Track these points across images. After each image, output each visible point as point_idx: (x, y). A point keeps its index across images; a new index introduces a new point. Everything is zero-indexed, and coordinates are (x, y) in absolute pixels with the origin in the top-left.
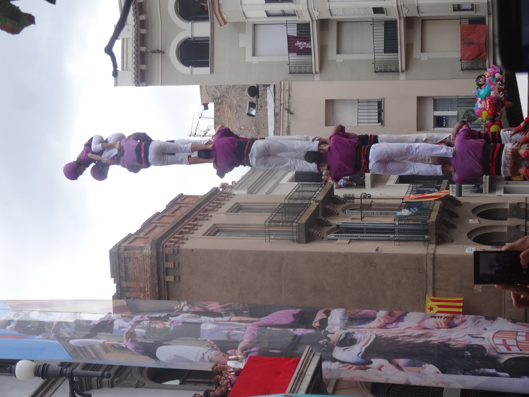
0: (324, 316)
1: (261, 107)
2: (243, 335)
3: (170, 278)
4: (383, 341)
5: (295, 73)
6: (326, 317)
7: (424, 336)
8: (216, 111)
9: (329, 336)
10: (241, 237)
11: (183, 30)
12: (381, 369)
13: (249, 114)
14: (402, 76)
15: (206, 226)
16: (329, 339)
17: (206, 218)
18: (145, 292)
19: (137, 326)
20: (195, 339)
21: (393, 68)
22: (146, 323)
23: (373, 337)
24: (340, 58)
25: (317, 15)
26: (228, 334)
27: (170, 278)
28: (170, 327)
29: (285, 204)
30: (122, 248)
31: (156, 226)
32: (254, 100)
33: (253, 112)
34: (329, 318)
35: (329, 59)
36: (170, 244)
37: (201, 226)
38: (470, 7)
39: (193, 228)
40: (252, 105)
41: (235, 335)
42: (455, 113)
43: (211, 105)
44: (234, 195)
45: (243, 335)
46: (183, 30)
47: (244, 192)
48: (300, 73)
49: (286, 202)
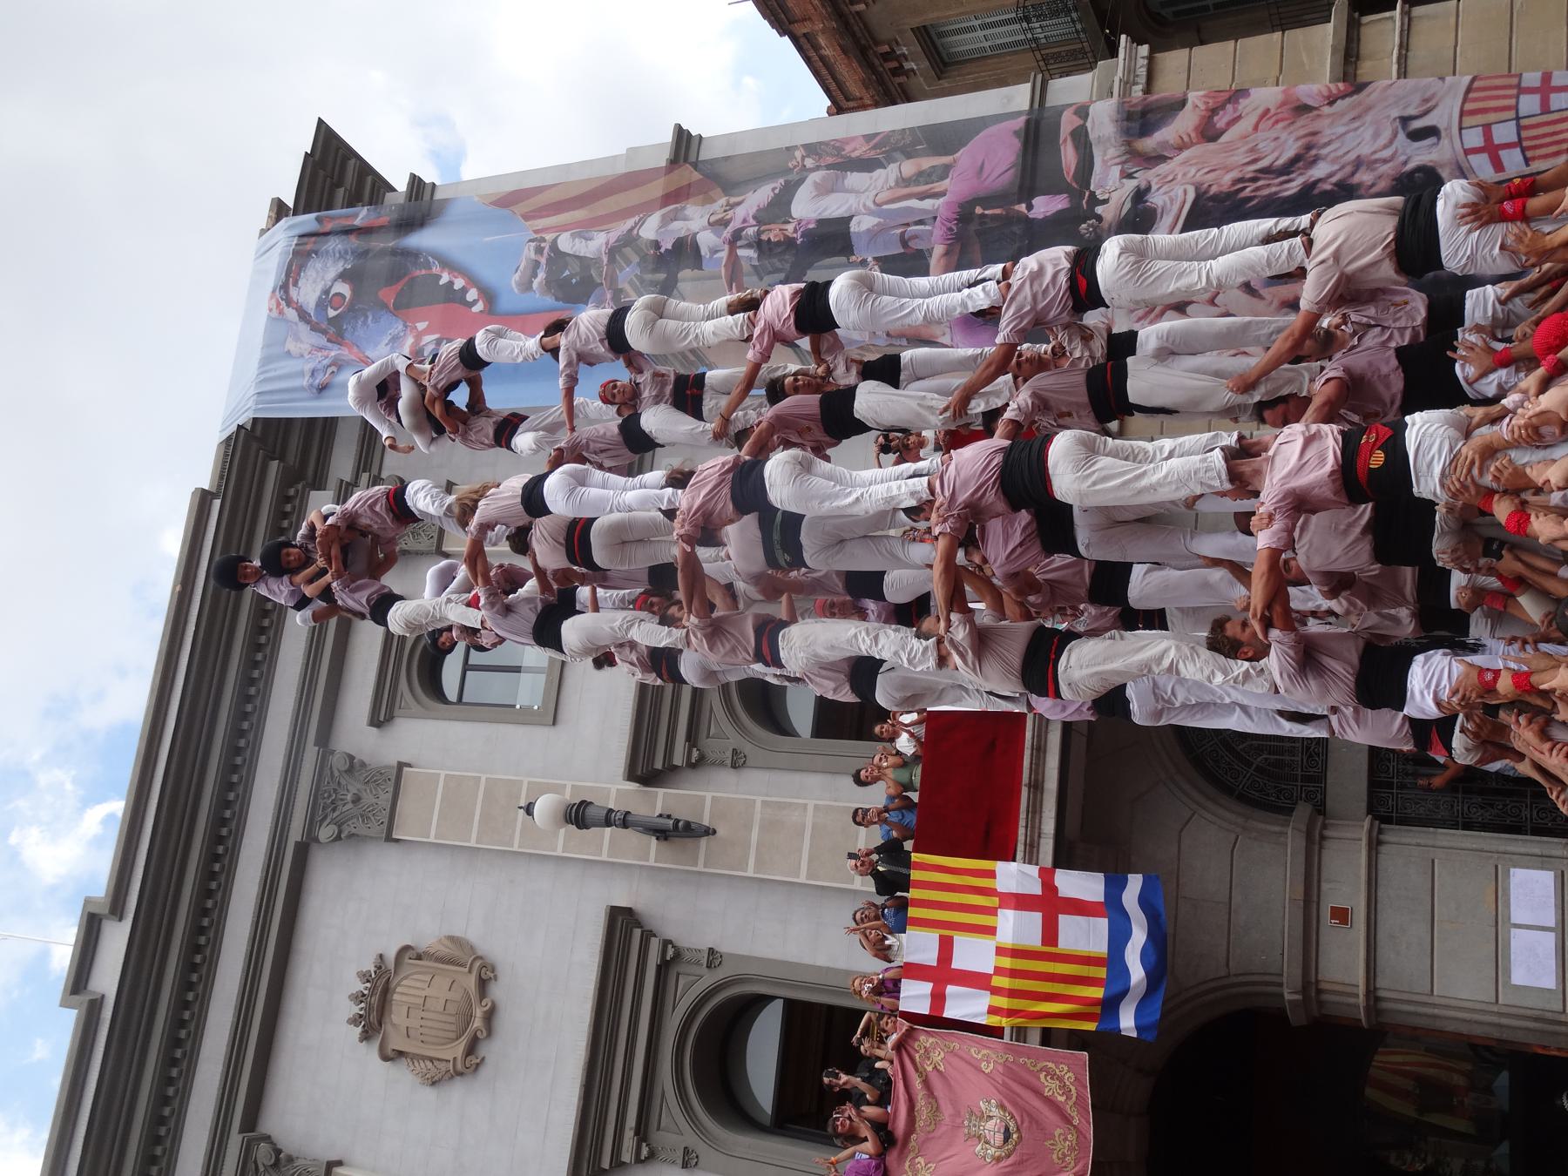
0: (1078, 122)
2: (931, 233)
4: (1211, 204)
6: (1082, 122)
7: (1301, 164)
9: (1099, 210)
12: (1216, 301)
16: (1099, 218)
19: (739, 243)
20: (843, 259)
22: (751, 231)
23: (1191, 196)
26: (903, 234)
28: (795, 235)
34: (1089, 124)
41: (915, 237)
45: (931, 233)
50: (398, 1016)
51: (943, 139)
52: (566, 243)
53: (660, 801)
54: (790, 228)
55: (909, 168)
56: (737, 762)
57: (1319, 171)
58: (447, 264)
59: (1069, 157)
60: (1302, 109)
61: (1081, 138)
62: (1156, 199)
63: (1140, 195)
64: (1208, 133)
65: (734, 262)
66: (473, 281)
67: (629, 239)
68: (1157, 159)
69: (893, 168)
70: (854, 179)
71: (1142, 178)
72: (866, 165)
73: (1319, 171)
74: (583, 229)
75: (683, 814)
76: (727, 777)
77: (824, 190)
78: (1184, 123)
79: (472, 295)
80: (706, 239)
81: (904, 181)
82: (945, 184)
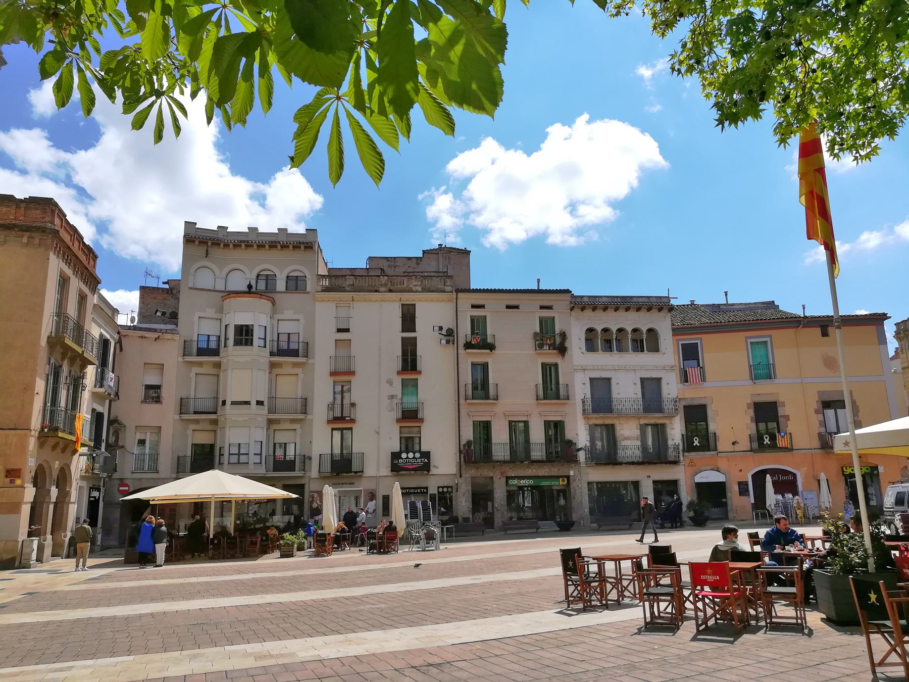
1: (163, 320)
3: (25, 240)
5: (185, 344)
8: (163, 289)
10: (57, 295)
11: (221, 272)
13: (157, 311)
14: (177, 417)
15: (69, 272)
17: (75, 272)
18: (15, 219)
21: (183, 411)
24: (193, 375)
25: (224, 361)
27: (25, 240)
29: (83, 329)
30: (54, 208)
31: (71, 236)
32: (167, 315)
33: (159, 314)
35: (193, 368)
36: (55, 243)
37: (69, 267)
38: (221, 462)
39: (68, 262)
40: (164, 314)
42: (147, 451)
43: (167, 286)
44: (94, 294)
46: (221, 272)
47: (95, 302)
48: (184, 348)
49: (85, 331)
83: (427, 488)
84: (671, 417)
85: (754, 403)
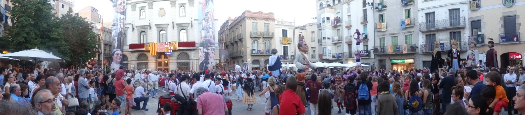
50: (161, 10)
51: (214, 38)
52: (209, 14)
53: (175, 26)
54: (209, 29)
55: (212, 36)
56: (178, 30)
57: (210, 58)
58: (208, 4)
59: (212, 45)
60: (213, 57)
61: (213, 46)
62: (209, 50)
63: (209, 50)
64: (213, 53)
65: (207, 26)
66: (207, 6)
67: (209, 18)
68: (211, 50)
69: (212, 35)
70: (212, 33)
71: (210, 50)
72: (213, 34)
73: (210, 58)
74: (210, 15)
75: (174, 27)
76: (177, 29)
77: (212, 31)
78: (213, 52)
79: (206, 6)
80: (209, 24)
81: (212, 36)
82: (211, 38)
83: (370, 63)
84: (463, 28)
85: (504, 17)
